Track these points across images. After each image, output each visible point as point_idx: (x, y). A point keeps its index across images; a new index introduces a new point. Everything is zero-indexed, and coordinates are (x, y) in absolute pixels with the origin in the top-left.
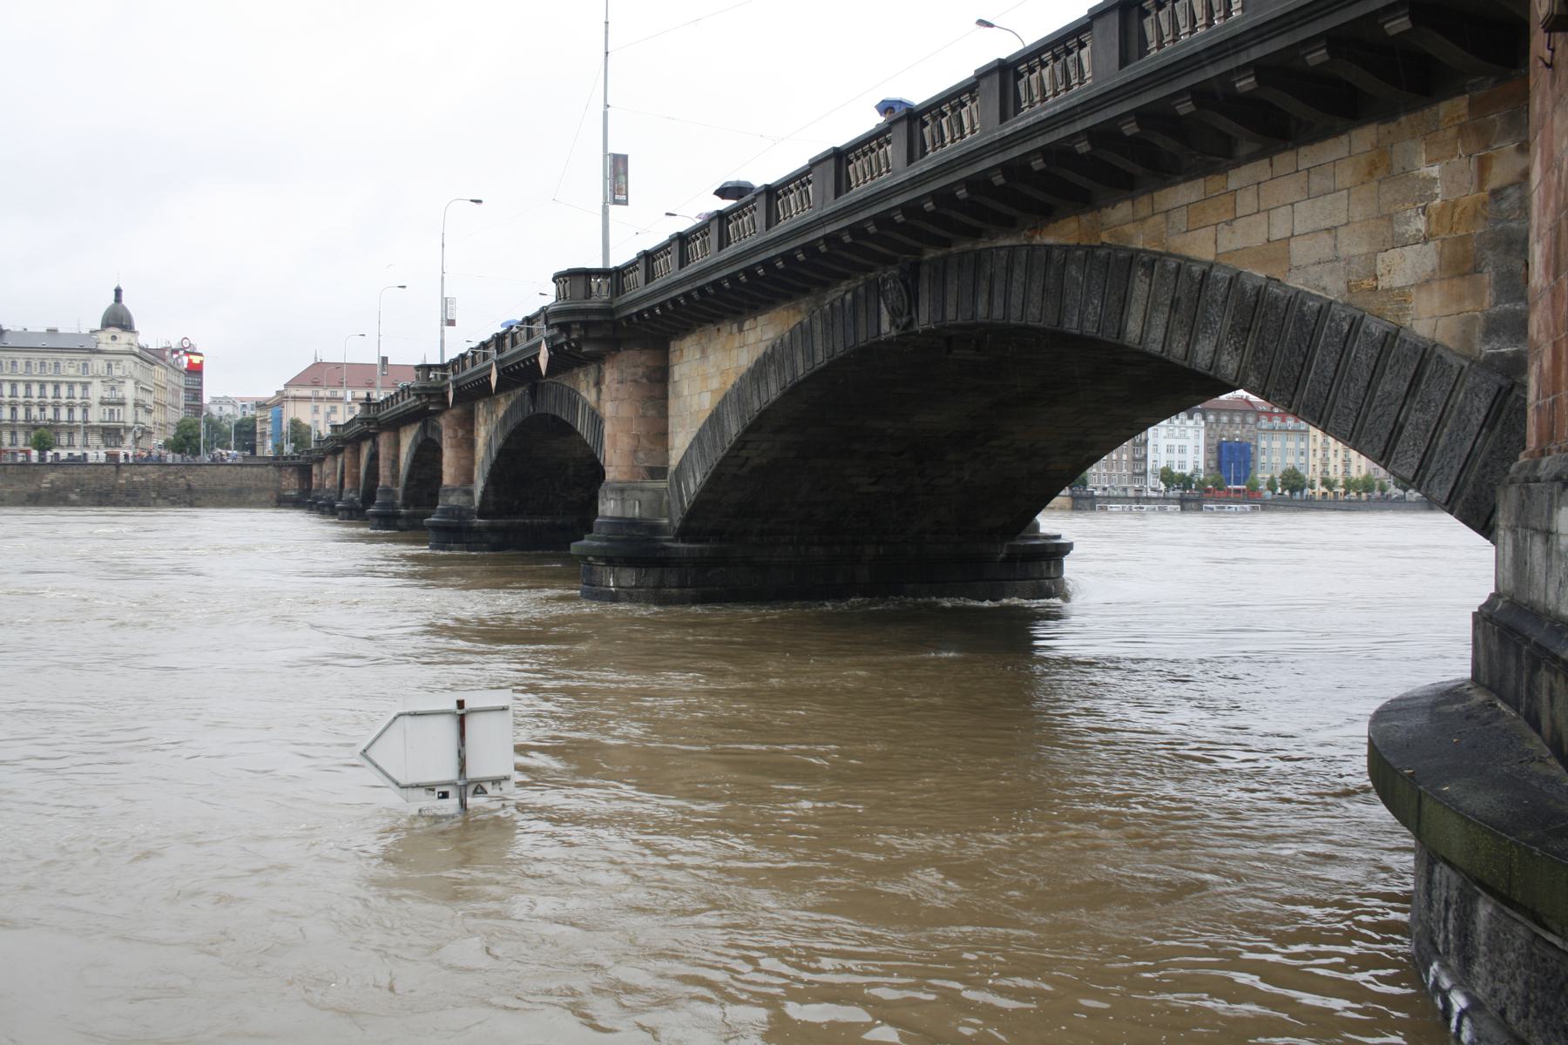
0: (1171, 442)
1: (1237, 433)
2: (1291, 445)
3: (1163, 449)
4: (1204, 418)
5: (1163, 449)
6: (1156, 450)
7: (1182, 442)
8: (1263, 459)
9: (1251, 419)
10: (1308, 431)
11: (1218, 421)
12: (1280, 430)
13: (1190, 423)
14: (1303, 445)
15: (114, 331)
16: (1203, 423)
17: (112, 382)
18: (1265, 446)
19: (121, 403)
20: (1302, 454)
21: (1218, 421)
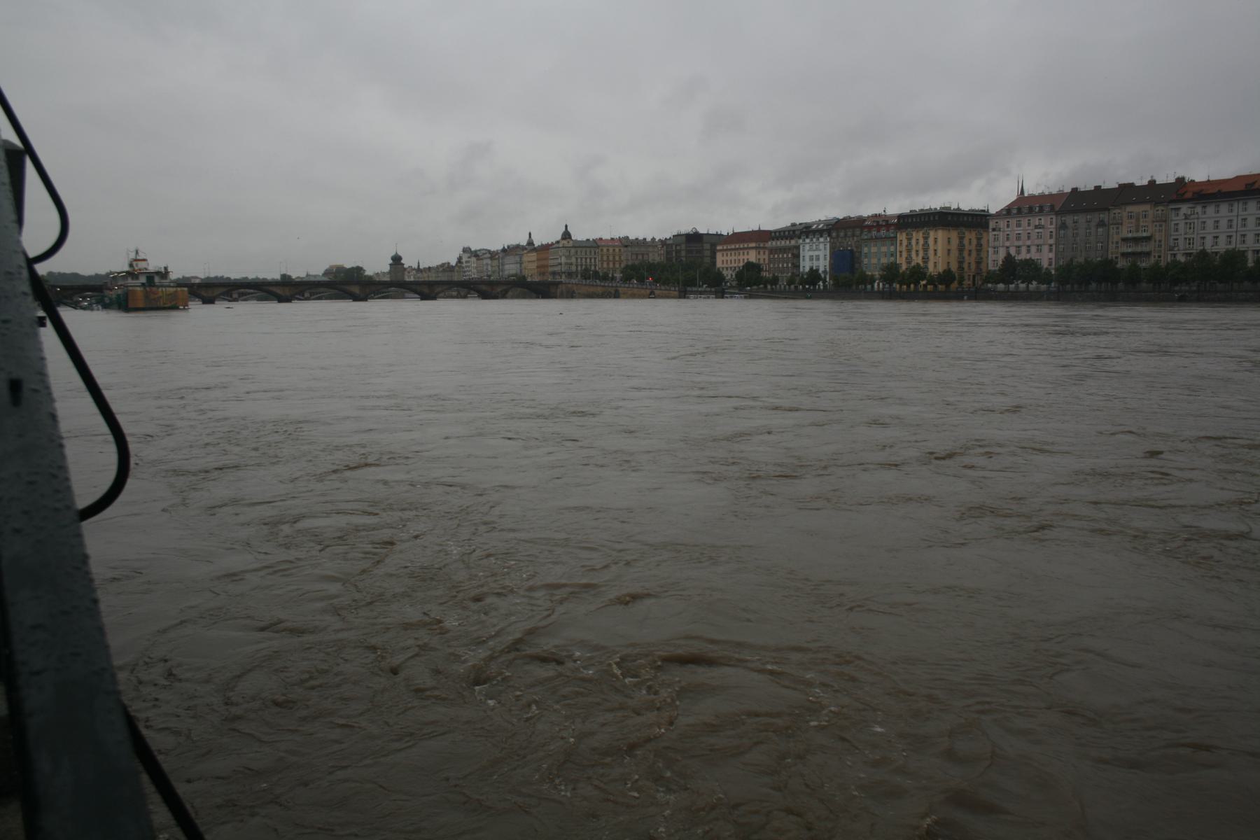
0: (811, 253)
1: (850, 243)
2: (884, 249)
3: (807, 259)
4: (829, 235)
5: (807, 259)
6: (804, 260)
7: (817, 253)
8: (866, 261)
9: (858, 232)
10: (896, 237)
11: (838, 236)
12: (876, 238)
13: (821, 240)
14: (892, 249)
15: (568, 240)
16: (828, 239)
17: (568, 257)
18: (866, 252)
19: (571, 264)
20: (892, 255)
21: (838, 236)
